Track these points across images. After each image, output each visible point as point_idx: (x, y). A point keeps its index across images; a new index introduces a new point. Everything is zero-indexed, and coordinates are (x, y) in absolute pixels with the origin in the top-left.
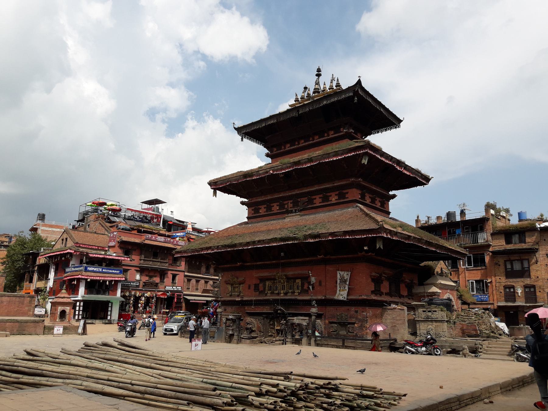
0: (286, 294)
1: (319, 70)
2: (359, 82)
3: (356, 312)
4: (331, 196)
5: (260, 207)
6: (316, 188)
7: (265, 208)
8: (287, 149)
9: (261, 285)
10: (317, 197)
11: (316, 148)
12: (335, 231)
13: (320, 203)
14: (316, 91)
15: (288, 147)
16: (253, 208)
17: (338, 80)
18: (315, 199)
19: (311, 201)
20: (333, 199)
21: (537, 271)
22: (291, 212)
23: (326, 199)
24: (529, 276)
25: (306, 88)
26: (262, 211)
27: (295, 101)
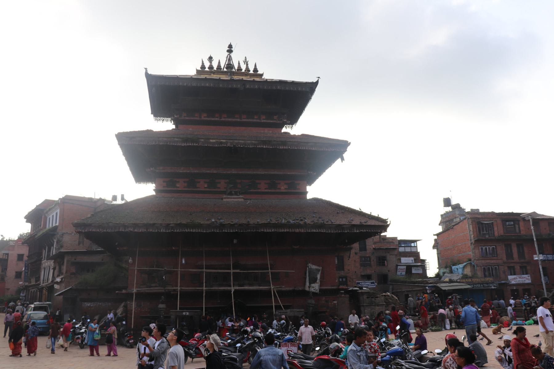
1: (230, 46)
2: (317, 83)
4: (279, 184)
6: (261, 172)
7: (185, 182)
8: (203, 118)
11: (243, 128)
12: (342, 223)
13: (266, 189)
14: (230, 66)
15: (204, 117)
17: (255, 65)
20: (282, 188)
22: (231, 194)
24: (343, 270)
25: (210, 59)
27: (201, 68)
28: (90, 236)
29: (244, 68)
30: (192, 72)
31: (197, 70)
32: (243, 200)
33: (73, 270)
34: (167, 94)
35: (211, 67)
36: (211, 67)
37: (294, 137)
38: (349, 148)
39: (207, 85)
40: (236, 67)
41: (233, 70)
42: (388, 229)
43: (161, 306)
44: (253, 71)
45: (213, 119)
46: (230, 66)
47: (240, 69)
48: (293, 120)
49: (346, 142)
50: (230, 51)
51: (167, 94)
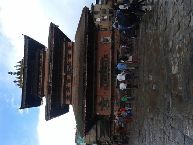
0: (109, 70)
1: (9, 73)
2: (25, 36)
3: (117, 35)
4: (69, 53)
5: (66, 95)
7: (67, 92)
8: (41, 85)
9: (105, 85)
10: (68, 60)
16: (66, 99)
18: (69, 62)
19: (69, 64)
20: (71, 52)
21: (105, 26)
22: (73, 74)
23: (69, 56)
24: (107, 28)
26: (68, 94)
28: (88, 130)
29: (19, 67)
30: (21, 90)
31: (20, 87)
32: (75, 69)
33: (103, 137)
34: (30, 100)
35: (19, 81)
36: (19, 81)
37: (49, 46)
38: (53, 23)
39: (26, 83)
40: (19, 71)
41: (20, 72)
42: (88, 7)
43: (115, 102)
44: (21, 63)
45: (41, 80)
46: (18, 73)
47: (19, 69)
48: (44, 47)
49: (50, 24)
50: (11, 73)
51: (30, 100)
